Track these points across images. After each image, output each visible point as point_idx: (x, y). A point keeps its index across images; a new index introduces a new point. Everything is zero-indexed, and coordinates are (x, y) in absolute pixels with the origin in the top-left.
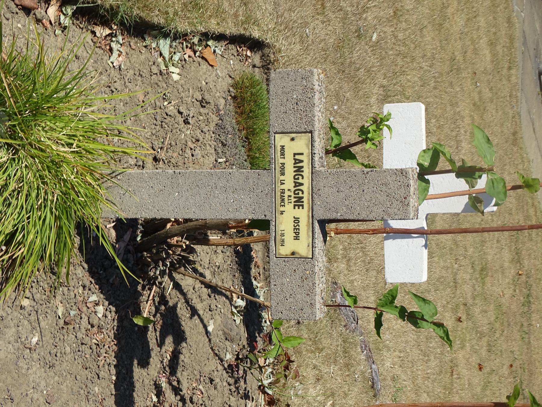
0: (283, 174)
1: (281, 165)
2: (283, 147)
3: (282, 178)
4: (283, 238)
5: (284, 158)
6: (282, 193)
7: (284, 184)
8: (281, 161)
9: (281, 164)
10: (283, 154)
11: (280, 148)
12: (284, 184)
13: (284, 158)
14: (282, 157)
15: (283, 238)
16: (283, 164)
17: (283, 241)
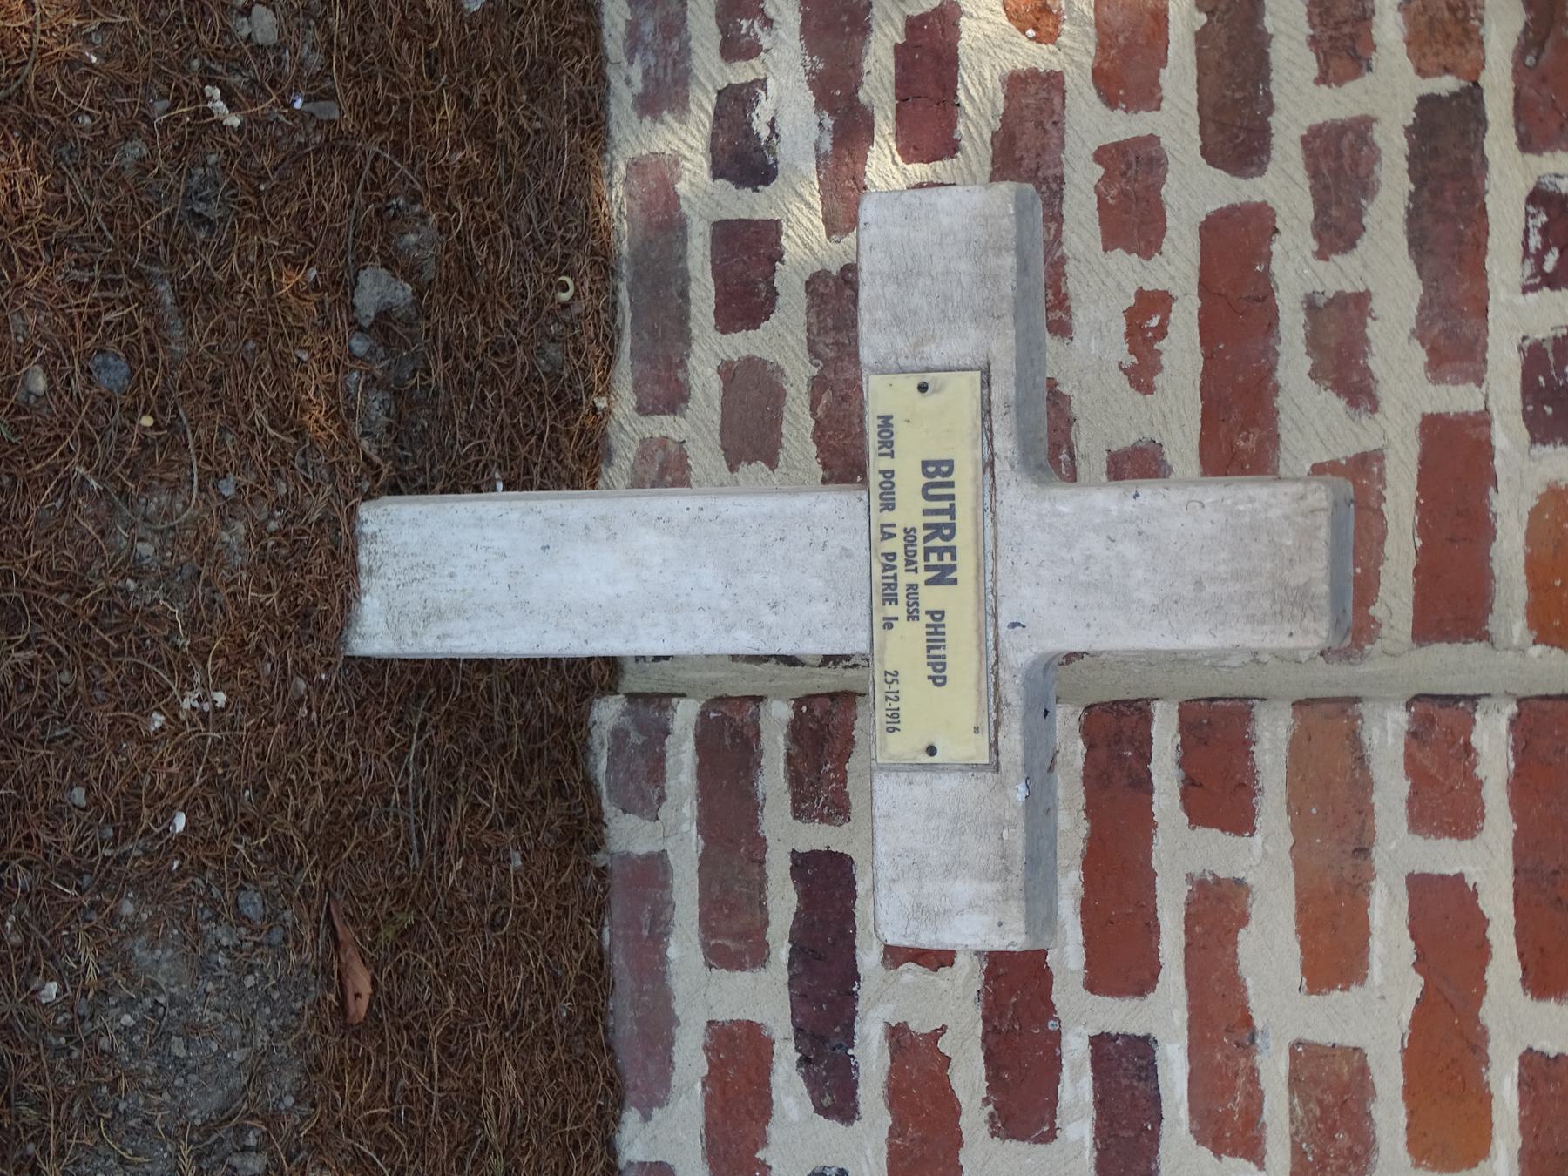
0: (889, 506)
1: (881, 478)
2: (886, 421)
3: (888, 517)
4: (895, 705)
5: (892, 455)
6: (886, 568)
7: (892, 536)
8: (885, 463)
9: (883, 472)
10: (887, 443)
11: (879, 422)
12: (892, 536)
13: (892, 455)
14: (885, 450)
15: (895, 705)
16: (888, 475)
17: (895, 715)
